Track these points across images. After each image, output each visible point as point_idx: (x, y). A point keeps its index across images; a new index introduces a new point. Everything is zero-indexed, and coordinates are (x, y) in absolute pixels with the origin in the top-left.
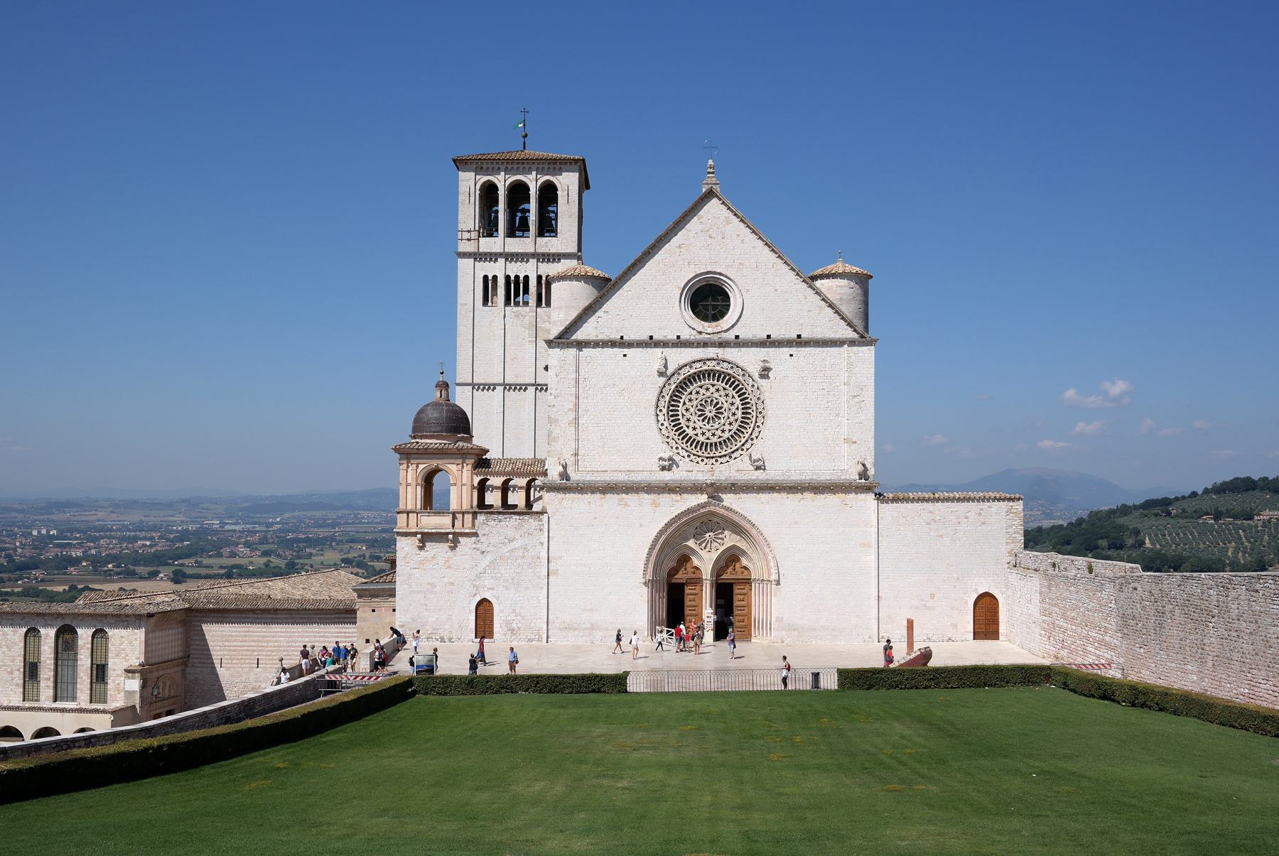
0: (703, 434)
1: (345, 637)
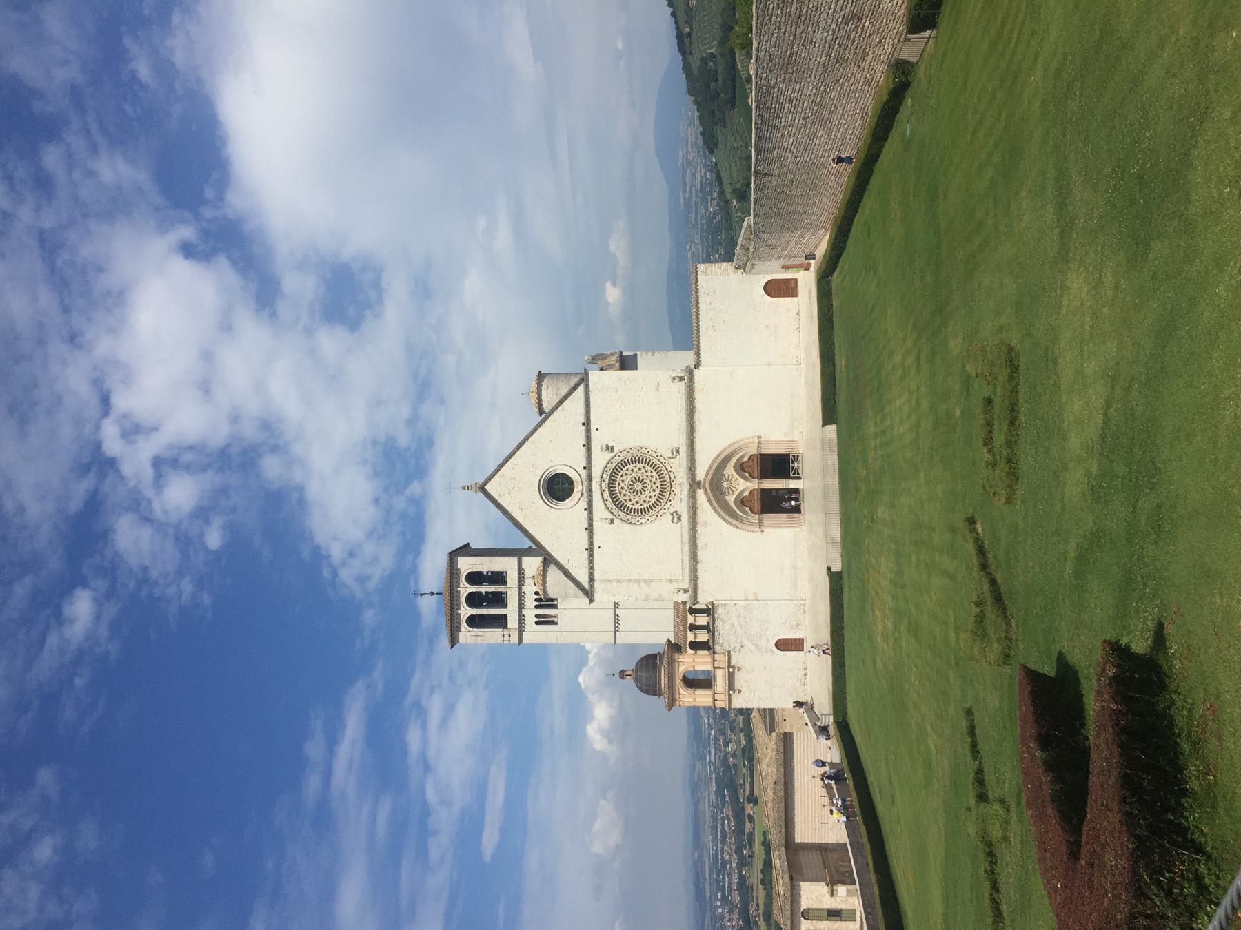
0: (654, 491)
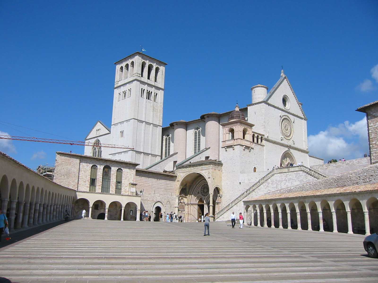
1: (166, 184)
